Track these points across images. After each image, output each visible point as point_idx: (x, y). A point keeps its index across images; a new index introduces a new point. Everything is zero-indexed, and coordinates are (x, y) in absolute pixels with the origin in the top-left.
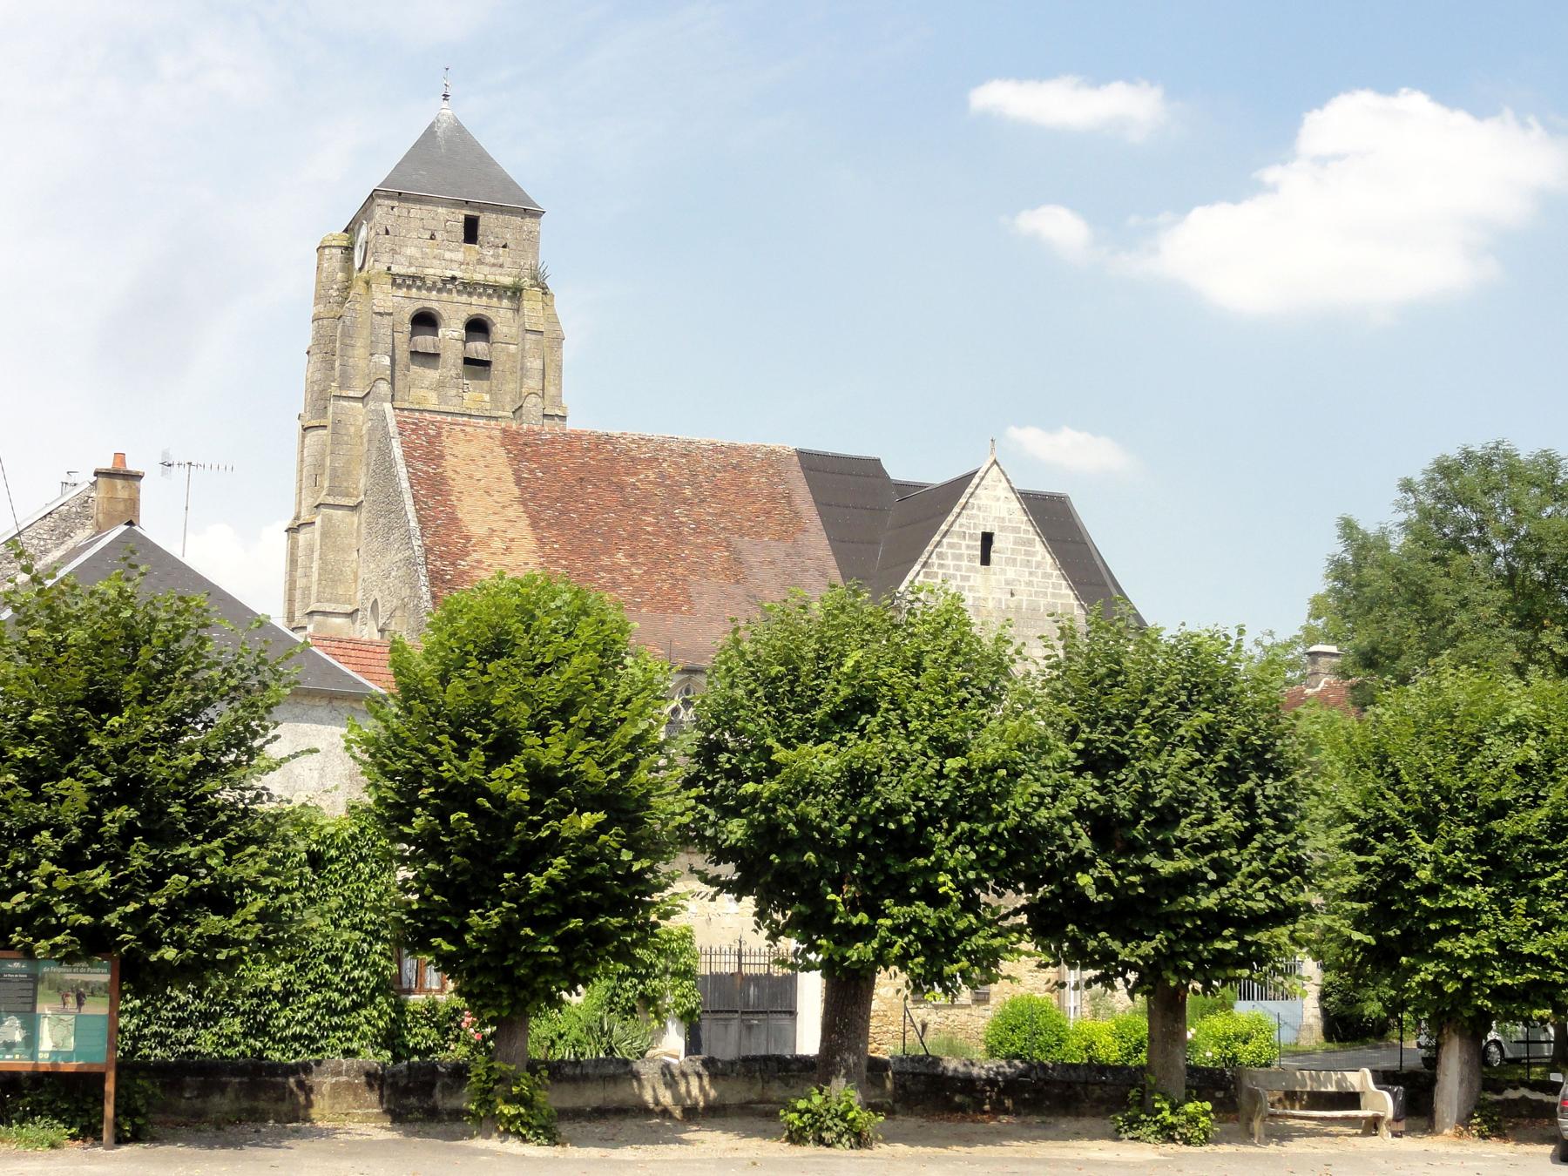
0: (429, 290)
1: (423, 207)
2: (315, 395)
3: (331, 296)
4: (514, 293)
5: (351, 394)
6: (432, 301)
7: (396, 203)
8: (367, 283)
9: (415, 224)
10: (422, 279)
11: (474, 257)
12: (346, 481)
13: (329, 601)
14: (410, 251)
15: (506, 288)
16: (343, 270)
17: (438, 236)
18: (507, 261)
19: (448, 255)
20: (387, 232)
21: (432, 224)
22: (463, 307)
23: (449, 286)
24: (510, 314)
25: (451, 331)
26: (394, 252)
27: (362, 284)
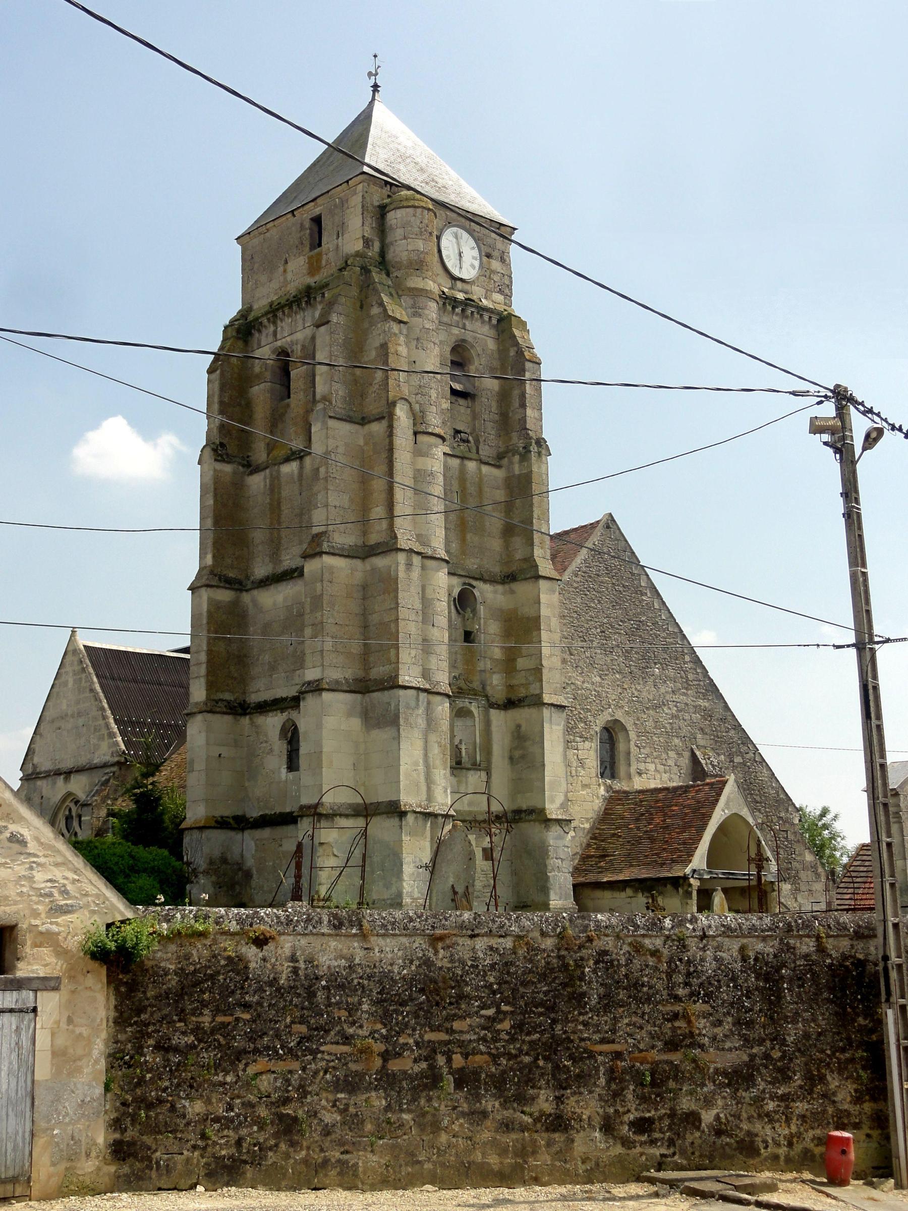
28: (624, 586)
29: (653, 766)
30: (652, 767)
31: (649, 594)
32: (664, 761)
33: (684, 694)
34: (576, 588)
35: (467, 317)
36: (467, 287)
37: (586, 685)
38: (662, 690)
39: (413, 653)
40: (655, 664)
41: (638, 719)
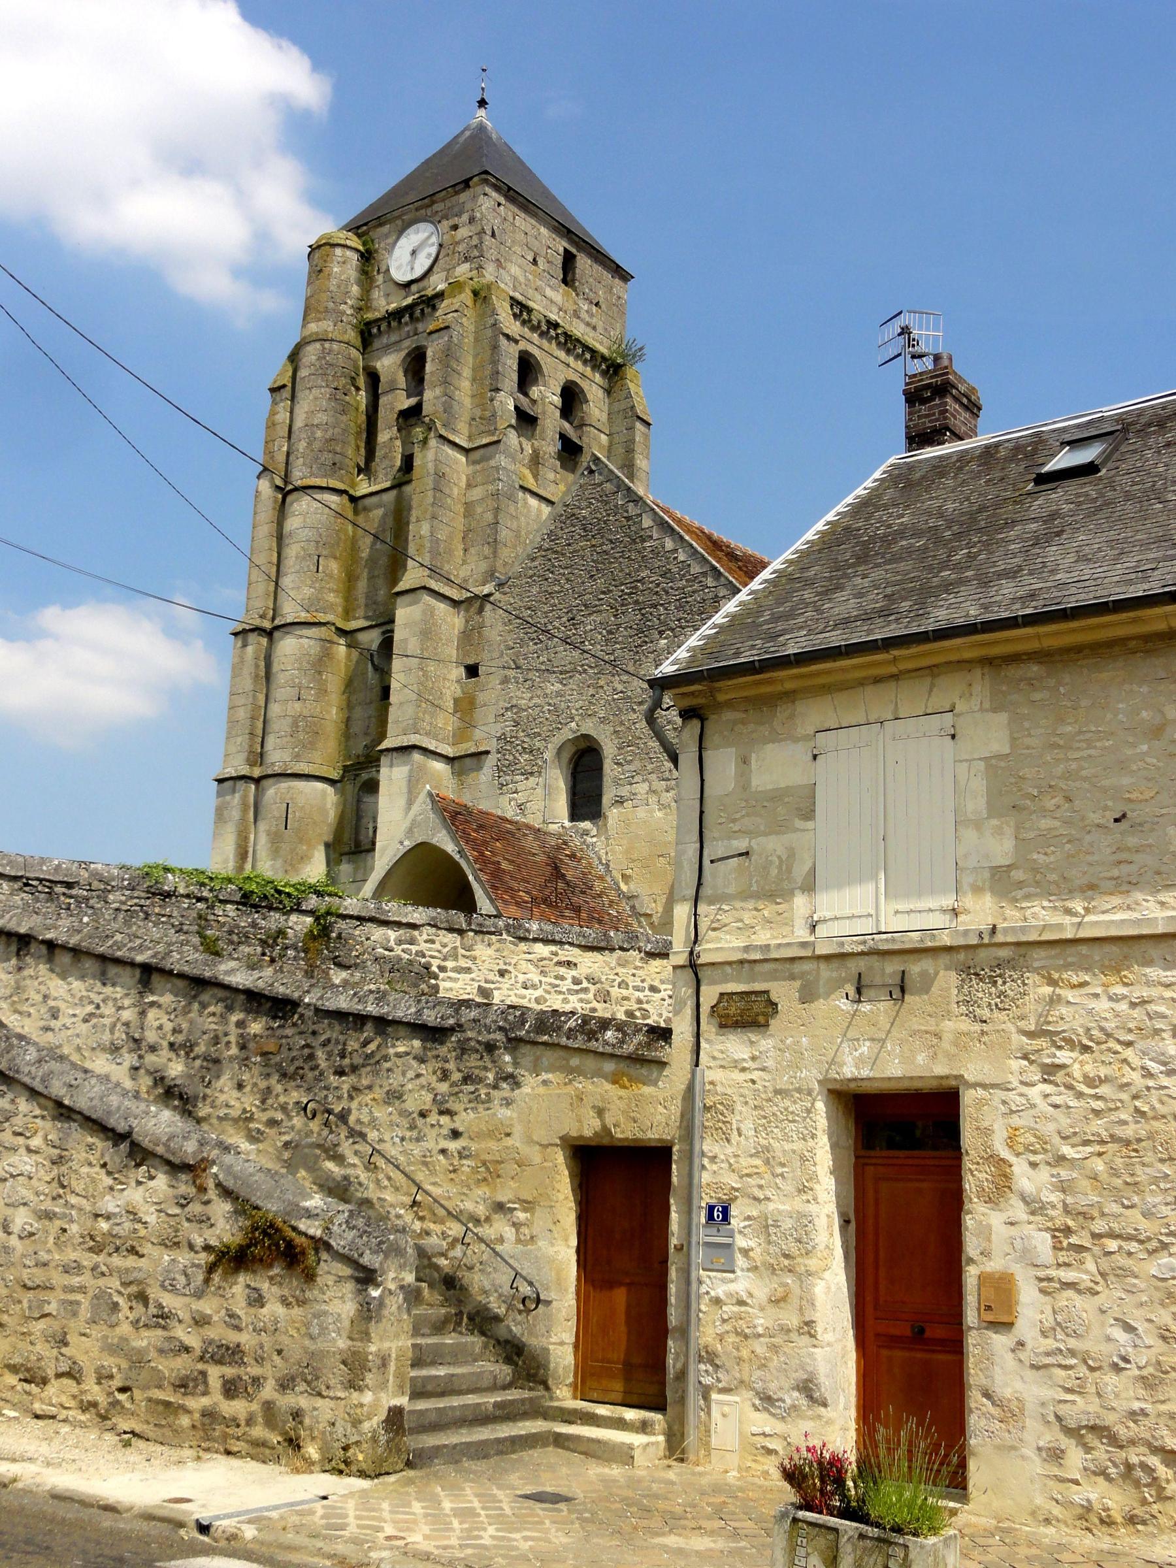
0: (534, 329)
1: (528, 219)
2: (317, 445)
3: (344, 313)
4: (608, 367)
5: (457, 441)
6: (537, 347)
7: (502, 200)
8: (475, 293)
10: (530, 310)
11: (570, 307)
12: (448, 562)
13: (427, 734)
14: (514, 270)
15: (604, 358)
16: (360, 283)
17: (540, 261)
18: (600, 326)
19: (549, 292)
20: (493, 235)
21: (535, 245)
22: (561, 367)
23: (552, 333)
24: (600, 393)
25: (548, 395)
26: (499, 264)
27: (466, 297)
28: (611, 541)
29: (646, 786)
30: (642, 788)
31: (655, 536)
32: (667, 775)
34: (531, 577)
35: (418, 320)
36: (421, 284)
37: (536, 701)
39: (239, 739)
40: (661, 633)
41: (622, 723)
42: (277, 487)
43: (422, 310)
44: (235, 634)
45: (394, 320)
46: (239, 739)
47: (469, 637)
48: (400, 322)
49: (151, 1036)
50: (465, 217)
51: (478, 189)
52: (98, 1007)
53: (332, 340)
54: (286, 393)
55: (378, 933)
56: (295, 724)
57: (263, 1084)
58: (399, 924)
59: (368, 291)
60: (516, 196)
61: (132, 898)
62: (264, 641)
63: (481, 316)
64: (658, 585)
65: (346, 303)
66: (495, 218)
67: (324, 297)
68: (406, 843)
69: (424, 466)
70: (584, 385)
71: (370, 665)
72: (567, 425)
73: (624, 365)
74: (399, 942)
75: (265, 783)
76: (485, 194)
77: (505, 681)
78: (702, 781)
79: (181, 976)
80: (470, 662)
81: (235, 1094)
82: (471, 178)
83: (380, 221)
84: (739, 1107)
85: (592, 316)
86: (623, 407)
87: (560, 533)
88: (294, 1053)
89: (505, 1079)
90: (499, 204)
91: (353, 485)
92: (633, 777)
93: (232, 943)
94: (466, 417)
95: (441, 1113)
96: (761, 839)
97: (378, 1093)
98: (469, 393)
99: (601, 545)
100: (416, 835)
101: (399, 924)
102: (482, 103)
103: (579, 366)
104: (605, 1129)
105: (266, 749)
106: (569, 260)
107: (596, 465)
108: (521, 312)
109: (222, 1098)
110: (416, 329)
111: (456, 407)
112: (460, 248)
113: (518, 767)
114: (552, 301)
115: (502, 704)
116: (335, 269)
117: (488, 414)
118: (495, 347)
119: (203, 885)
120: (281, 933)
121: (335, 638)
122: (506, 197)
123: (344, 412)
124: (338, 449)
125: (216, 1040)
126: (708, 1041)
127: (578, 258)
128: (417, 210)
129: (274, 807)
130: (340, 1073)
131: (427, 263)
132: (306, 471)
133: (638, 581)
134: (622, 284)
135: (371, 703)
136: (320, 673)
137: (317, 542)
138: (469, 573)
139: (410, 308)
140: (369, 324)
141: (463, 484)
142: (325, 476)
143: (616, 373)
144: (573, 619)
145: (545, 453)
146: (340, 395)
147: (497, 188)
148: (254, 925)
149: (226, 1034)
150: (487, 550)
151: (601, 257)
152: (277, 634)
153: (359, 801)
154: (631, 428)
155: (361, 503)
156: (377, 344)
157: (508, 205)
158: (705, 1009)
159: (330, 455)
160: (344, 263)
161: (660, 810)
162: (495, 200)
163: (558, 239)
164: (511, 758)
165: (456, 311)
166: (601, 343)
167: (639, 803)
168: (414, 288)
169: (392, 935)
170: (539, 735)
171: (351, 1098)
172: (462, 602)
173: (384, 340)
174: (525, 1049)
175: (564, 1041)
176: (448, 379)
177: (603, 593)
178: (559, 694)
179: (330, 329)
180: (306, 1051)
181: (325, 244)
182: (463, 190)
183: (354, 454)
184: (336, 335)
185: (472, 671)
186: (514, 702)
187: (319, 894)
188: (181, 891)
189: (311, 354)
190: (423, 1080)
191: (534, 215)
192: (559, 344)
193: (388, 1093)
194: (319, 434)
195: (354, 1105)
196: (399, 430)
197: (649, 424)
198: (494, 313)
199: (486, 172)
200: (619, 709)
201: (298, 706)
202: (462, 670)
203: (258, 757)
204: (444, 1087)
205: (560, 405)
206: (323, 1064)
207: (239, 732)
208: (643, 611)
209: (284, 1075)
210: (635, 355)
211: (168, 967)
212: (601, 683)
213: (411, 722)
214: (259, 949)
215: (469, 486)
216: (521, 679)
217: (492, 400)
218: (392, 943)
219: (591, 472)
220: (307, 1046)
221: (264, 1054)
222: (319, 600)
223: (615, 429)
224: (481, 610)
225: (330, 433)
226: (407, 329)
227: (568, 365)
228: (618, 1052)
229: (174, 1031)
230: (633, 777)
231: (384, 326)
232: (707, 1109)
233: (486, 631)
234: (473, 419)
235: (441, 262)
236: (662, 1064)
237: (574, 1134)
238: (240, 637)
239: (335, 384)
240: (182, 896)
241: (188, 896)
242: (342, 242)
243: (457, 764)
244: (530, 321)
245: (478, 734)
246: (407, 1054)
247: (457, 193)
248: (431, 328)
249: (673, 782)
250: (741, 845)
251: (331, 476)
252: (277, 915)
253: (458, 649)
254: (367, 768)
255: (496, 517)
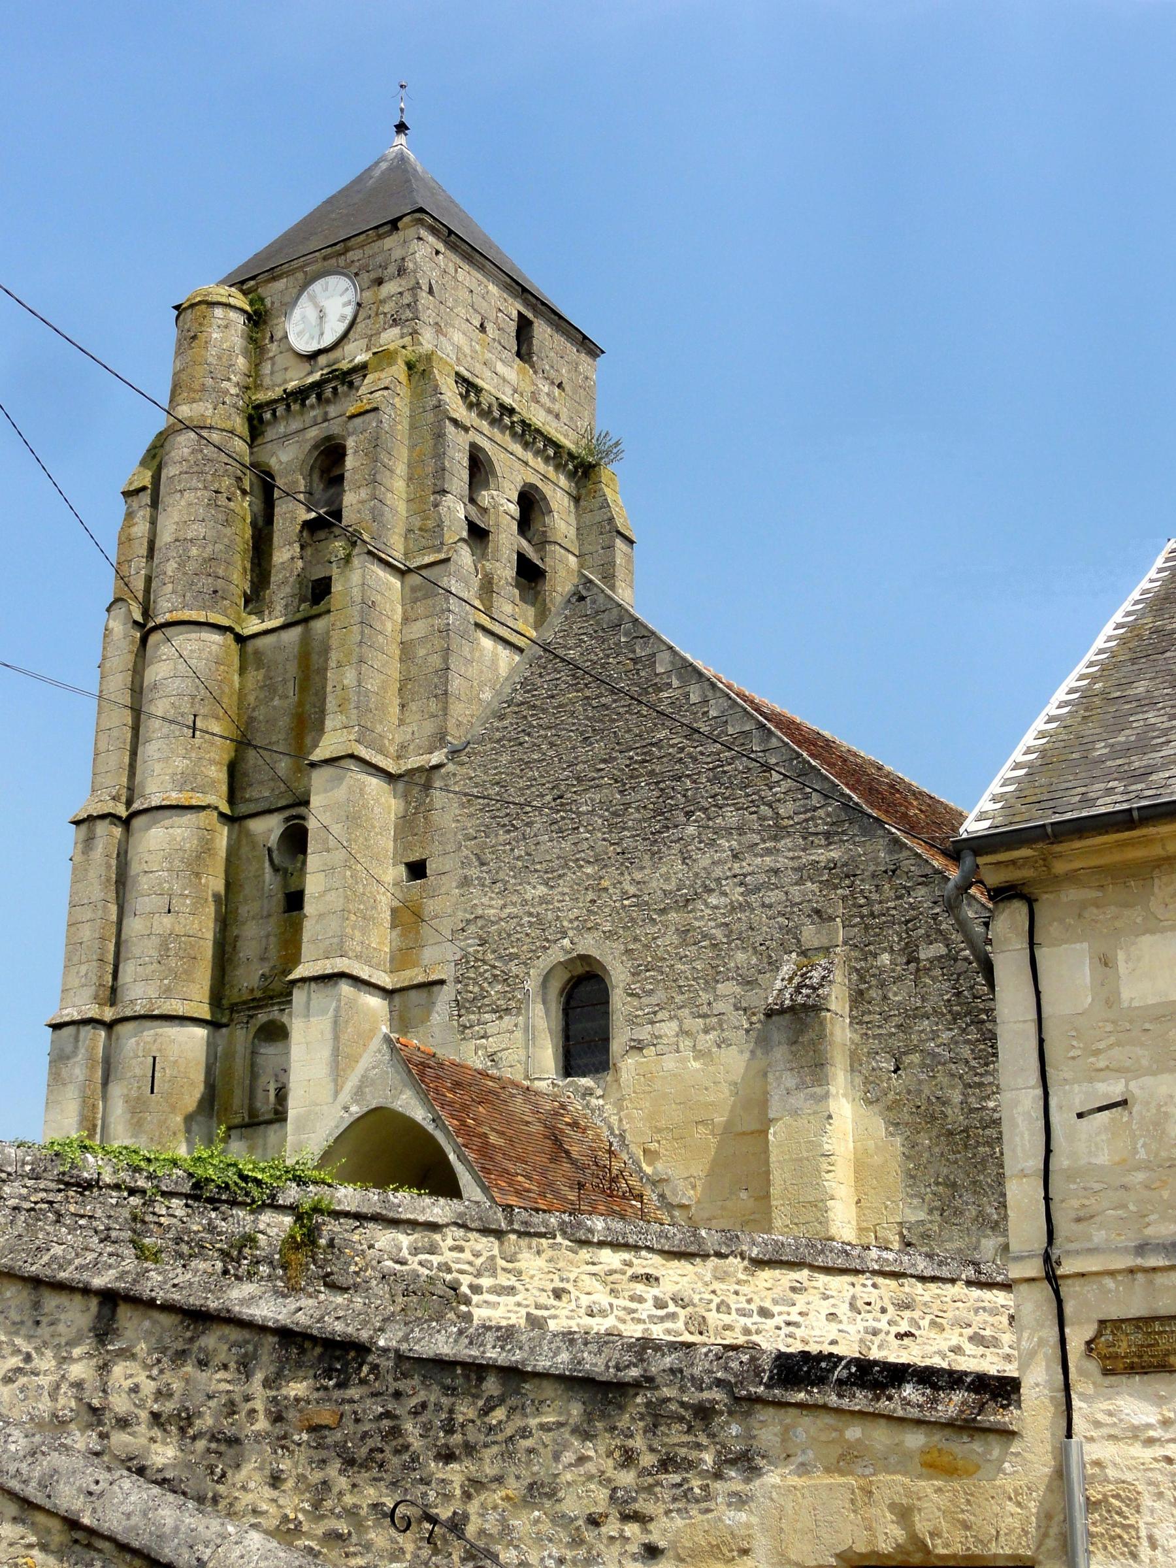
0: (484, 414)
1: (474, 273)
2: (191, 567)
3: (226, 392)
4: (576, 468)
7: (441, 247)
8: (410, 366)
9: (464, 294)
10: (478, 390)
11: (528, 389)
12: (381, 722)
13: (358, 957)
14: (458, 337)
15: (571, 456)
16: (246, 353)
17: (489, 327)
19: (500, 368)
21: (483, 306)
22: (518, 465)
23: (507, 420)
26: (438, 329)
27: (399, 370)
29: (674, 1025)
30: (669, 1029)
31: (675, 683)
32: (705, 1009)
33: (768, 852)
34: (498, 741)
35: (328, 401)
36: (332, 356)
38: (705, 861)
39: (83, 969)
40: (688, 814)
41: (636, 939)
42: (135, 622)
43: (335, 389)
44: (77, 823)
45: (295, 402)
46: (83, 969)
47: (407, 826)
48: (303, 405)
49: (120, 1404)
50: (392, 269)
51: (408, 231)
52: (28, 1358)
53: (211, 428)
54: (146, 498)
55: (385, 1238)
56: (164, 947)
57: (316, 1477)
58: (413, 1224)
59: (257, 365)
60: (459, 243)
61: (36, 1190)
62: (118, 831)
63: (417, 395)
64: (682, 750)
65: (229, 380)
66: (432, 270)
67: (199, 371)
68: (354, 1109)
69: (347, 592)
70: (547, 489)
71: (267, 864)
72: (524, 543)
73: (598, 464)
74: (415, 1251)
75: (124, 1029)
76: (420, 239)
77: (465, 882)
78: (1038, 993)
79: (169, 1308)
80: (413, 857)
81: (268, 1492)
82: (400, 218)
83: (273, 274)
84: (1147, 1501)
85: (553, 400)
86: (598, 519)
87: (539, 681)
88: (367, 1427)
89: (732, 1462)
90: (437, 253)
91: (239, 621)
92: (655, 1013)
93: (181, 1256)
94: (400, 529)
95: (626, 1518)
96: (1148, 1081)
97: (513, 1488)
98: (404, 496)
99: (597, 697)
100: (368, 1097)
101: (413, 1224)
102: (401, 128)
103: (538, 463)
104: (914, 1539)
105: (121, 981)
106: (524, 328)
107: (588, 590)
108: (468, 391)
109: (246, 1499)
110: (326, 413)
111: (388, 515)
112: (386, 308)
113: (486, 1001)
114: (504, 380)
115: (460, 915)
116: (215, 335)
117: (430, 524)
118: (440, 436)
119: (137, 1169)
120: (249, 1240)
121: (218, 826)
122: (446, 243)
123: (227, 523)
124: (221, 573)
125: (231, 1408)
126: (1084, 1397)
127: (536, 324)
128: (325, 258)
129: (134, 1062)
130: (447, 1456)
131: (341, 328)
132: (177, 600)
133: (652, 744)
134: (589, 360)
135: (269, 916)
136: (198, 875)
137: (193, 697)
138: (409, 737)
139: (318, 386)
140: (259, 407)
141: (398, 617)
142: (204, 608)
143: (586, 474)
144: (561, 797)
145: (500, 578)
146: (222, 500)
147: (433, 231)
148: (211, 1228)
149: (247, 1399)
150: (433, 706)
151: (563, 324)
152: (137, 823)
153: (254, 1053)
154: (611, 547)
155: (251, 646)
156: (271, 433)
157: (448, 253)
158: (1076, 1345)
159: (210, 580)
160: (226, 327)
161: (695, 1059)
162: (432, 247)
163: (510, 300)
164: (476, 989)
165: (386, 388)
166: (566, 436)
167: (666, 1049)
168: (322, 360)
169: (405, 1240)
170: (516, 956)
171: (467, 1496)
172: (401, 776)
173: (281, 429)
174: (765, 1414)
175: (833, 1400)
176: (378, 477)
177: (604, 761)
178: (543, 900)
179: (209, 413)
180: (386, 1423)
181: (200, 302)
182: (389, 233)
183: (239, 580)
184: (216, 421)
185: (417, 870)
186: (480, 912)
187: (300, 1181)
188: (108, 1179)
189: (184, 443)
190: (590, 1467)
191: (481, 268)
192: (514, 435)
193: (531, 1487)
194: (194, 551)
195: (473, 1508)
196: (302, 547)
197: (632, 542)
198: (436, 391)
199: (421, 210)
200: (632, 920)
201: (167, 920)
202: (402, 869)
203: (113, 995)
204: (627, 1478)
205: (517, 515)
206: (416, 1444)
207: (84, 958)
208: (662, 785)
209: (350, 1462)
210: (612, 451)
211: (146, 1294)
212: (605, 883)
213: (336, 940)
214: (219, 1265)
215: (406, 620)
216: (487, 882)
217: (436, 505)
218: (405, 1253)
219: (582, 598)
220: (387, 1415)
221: (314, 1429)
222: (195, 776)
223: (588, 548)
224: (427, 787)
225: (209, 549)
226: (313, 413)
227: (526, 463)
228: (930, 1416)
229: (159, 1394)
230: (655, 1013)
231: (281, 409)
232: (1091, 1505)
233: (435, 816)
234: (410, 531)
235: (360, 327)
236: (1008, 1434)
237: (861, 1548)
238: (84, 827)
239: (216, 486)
240: (108, 1186)
241: (117, 1187)
242: (224, 300)
243: (397, 999)
244: (479, 404)
245: (429, 954)
246: (560, 1425)
247: (380, 237)
248: (352, 410)
249: (715, 1020)
250: (1113, 1089)
251: (211, 608)
252: (241, 1214)
253: (395, 840)
254: (266, 1006)
255: (446, 660)
